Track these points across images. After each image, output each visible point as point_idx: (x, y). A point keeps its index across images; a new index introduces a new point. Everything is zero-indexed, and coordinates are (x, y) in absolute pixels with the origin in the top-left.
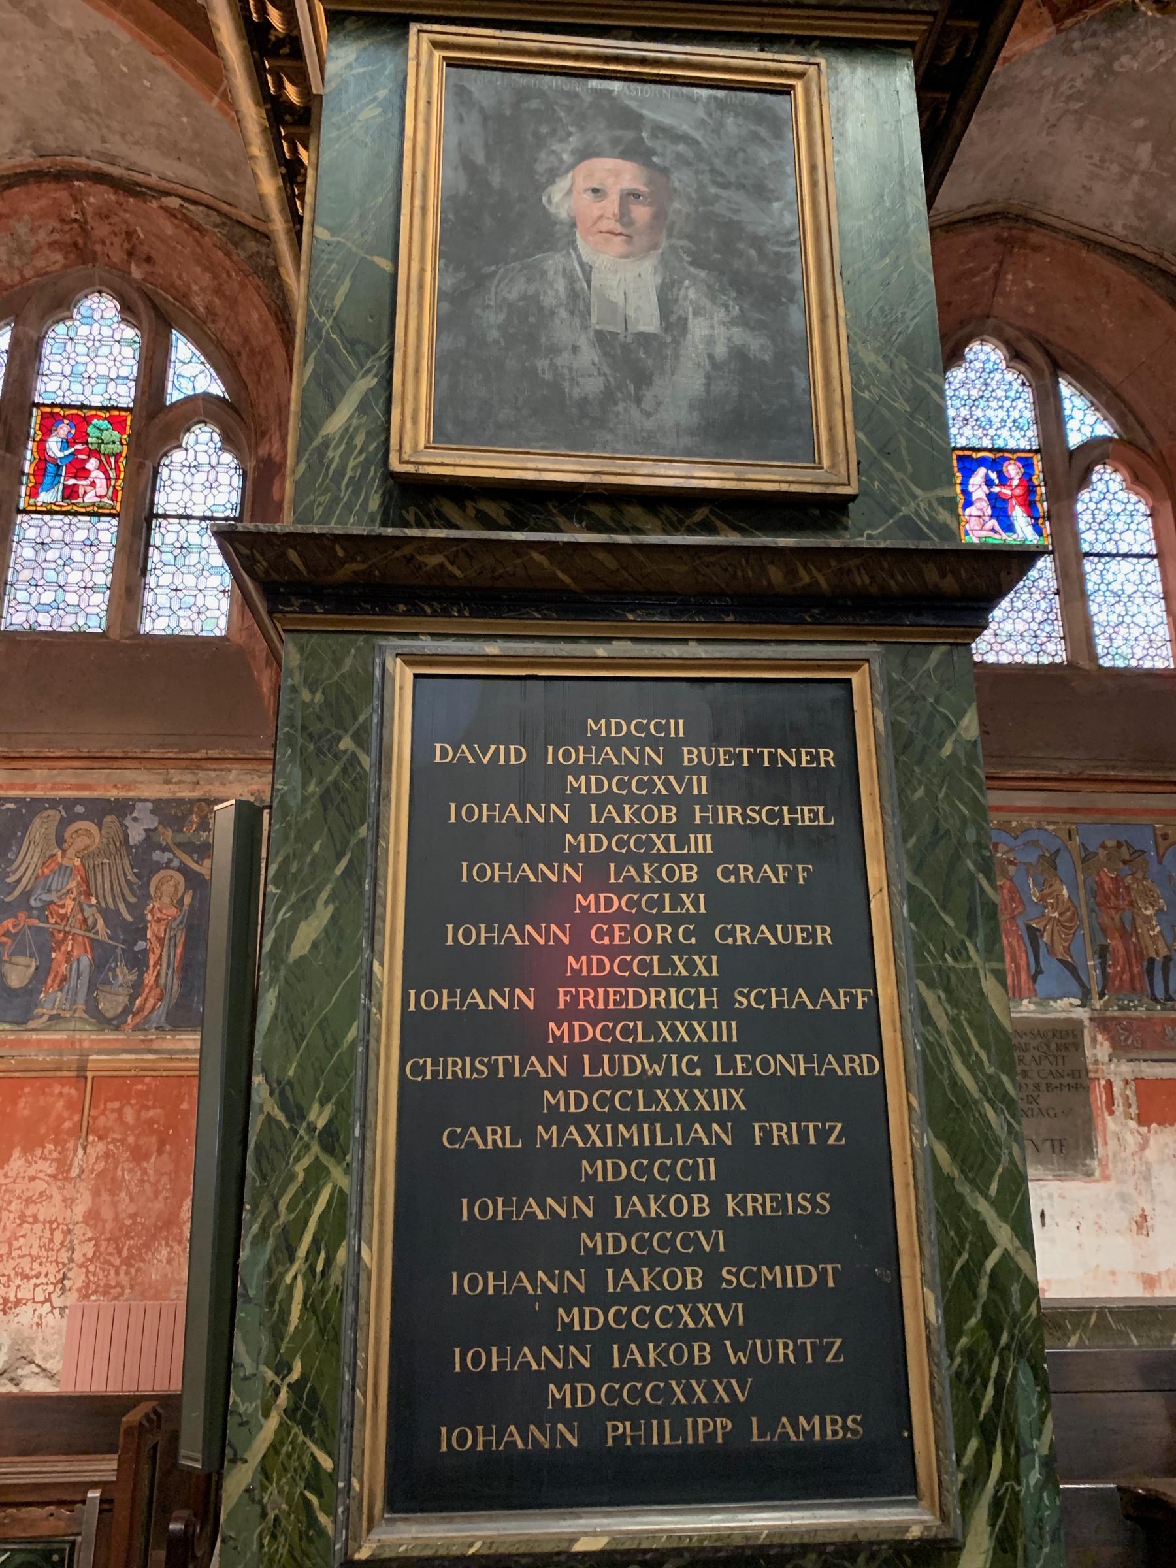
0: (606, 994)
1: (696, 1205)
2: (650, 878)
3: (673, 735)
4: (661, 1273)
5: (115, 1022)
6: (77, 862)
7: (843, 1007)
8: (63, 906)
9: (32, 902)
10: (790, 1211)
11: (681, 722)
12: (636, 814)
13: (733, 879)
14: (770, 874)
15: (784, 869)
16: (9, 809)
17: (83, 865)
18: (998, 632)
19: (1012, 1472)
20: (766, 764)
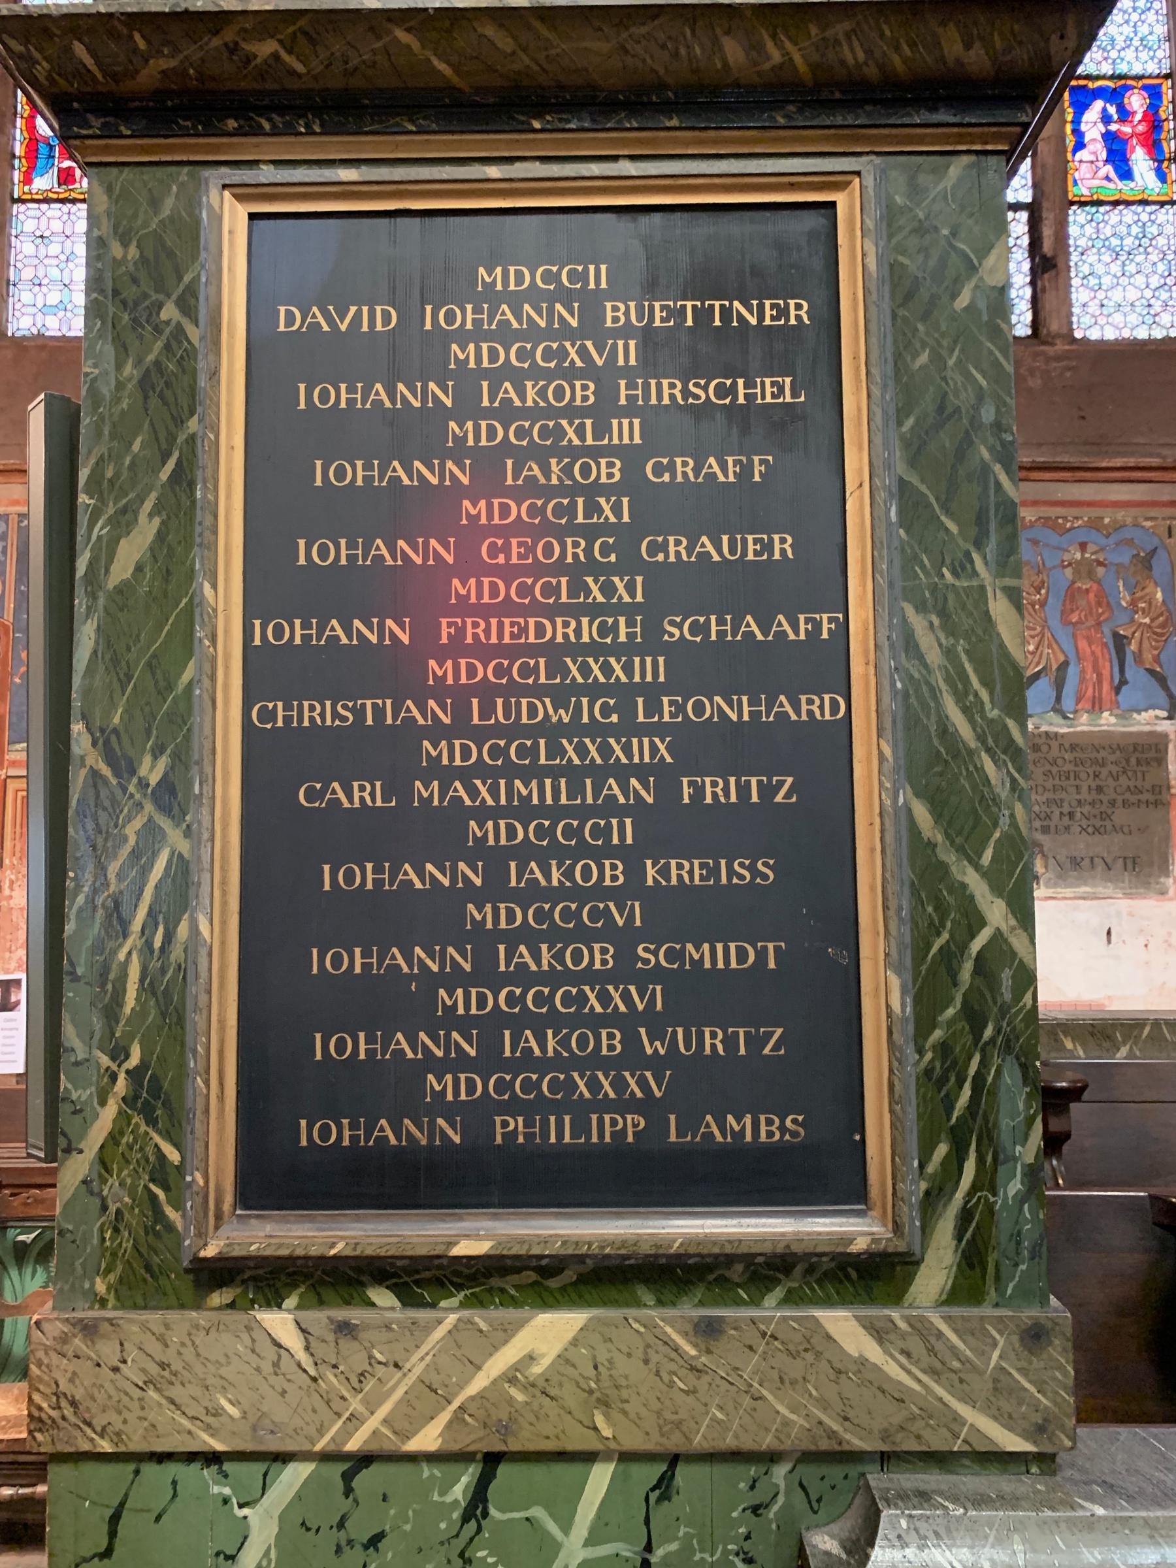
0: (501, 625)
1: (608, 873)
2: (559, 478)
3: (592, 286)
4: (564, 950)
7: (802, 637)
10: (724, 880)
11: (603, 267)
12: (542, 393)
13: (666, 477)
14: (716, 469)
15: (735, 463)
18: (1105, 302)
19: (987, 1181)
20: (717, 323)
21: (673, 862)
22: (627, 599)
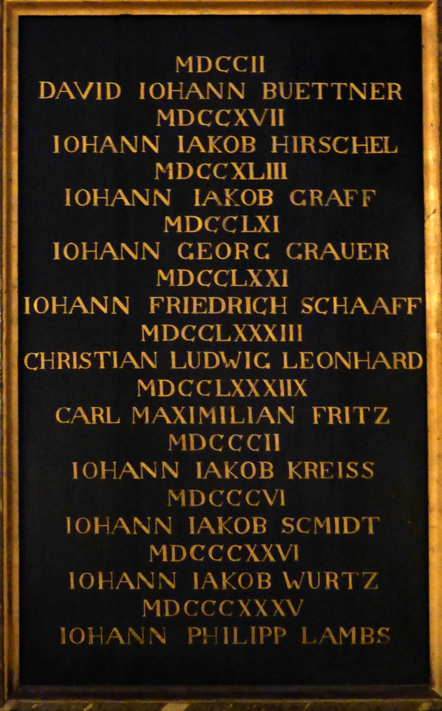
0: (191, 302)
1: (263, 470)
2: (231, 202)
3: (254, 70)
4: (233, 520)
7: (395, 312)
11: (262, 58)
13: (304, 203)
14: (338, 198)
15: (351, 194)
20: (339, 98)
21: (307, 464)
22: (277, 285)
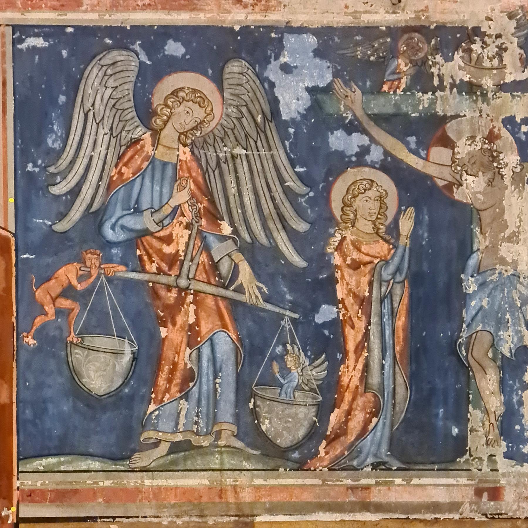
5: (296, 455)
6: (185, 154)
8: (168, 240)
9: (109, 234)
16: (34, 50)
17: (198, 160)
